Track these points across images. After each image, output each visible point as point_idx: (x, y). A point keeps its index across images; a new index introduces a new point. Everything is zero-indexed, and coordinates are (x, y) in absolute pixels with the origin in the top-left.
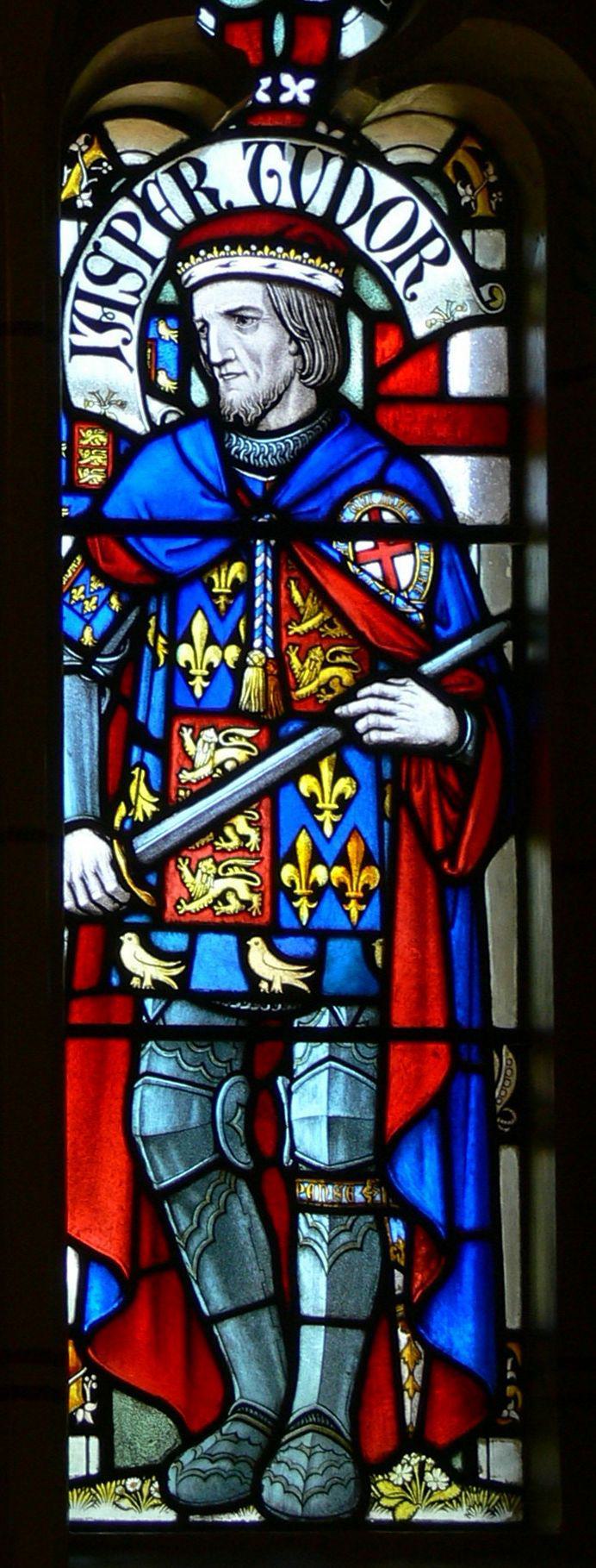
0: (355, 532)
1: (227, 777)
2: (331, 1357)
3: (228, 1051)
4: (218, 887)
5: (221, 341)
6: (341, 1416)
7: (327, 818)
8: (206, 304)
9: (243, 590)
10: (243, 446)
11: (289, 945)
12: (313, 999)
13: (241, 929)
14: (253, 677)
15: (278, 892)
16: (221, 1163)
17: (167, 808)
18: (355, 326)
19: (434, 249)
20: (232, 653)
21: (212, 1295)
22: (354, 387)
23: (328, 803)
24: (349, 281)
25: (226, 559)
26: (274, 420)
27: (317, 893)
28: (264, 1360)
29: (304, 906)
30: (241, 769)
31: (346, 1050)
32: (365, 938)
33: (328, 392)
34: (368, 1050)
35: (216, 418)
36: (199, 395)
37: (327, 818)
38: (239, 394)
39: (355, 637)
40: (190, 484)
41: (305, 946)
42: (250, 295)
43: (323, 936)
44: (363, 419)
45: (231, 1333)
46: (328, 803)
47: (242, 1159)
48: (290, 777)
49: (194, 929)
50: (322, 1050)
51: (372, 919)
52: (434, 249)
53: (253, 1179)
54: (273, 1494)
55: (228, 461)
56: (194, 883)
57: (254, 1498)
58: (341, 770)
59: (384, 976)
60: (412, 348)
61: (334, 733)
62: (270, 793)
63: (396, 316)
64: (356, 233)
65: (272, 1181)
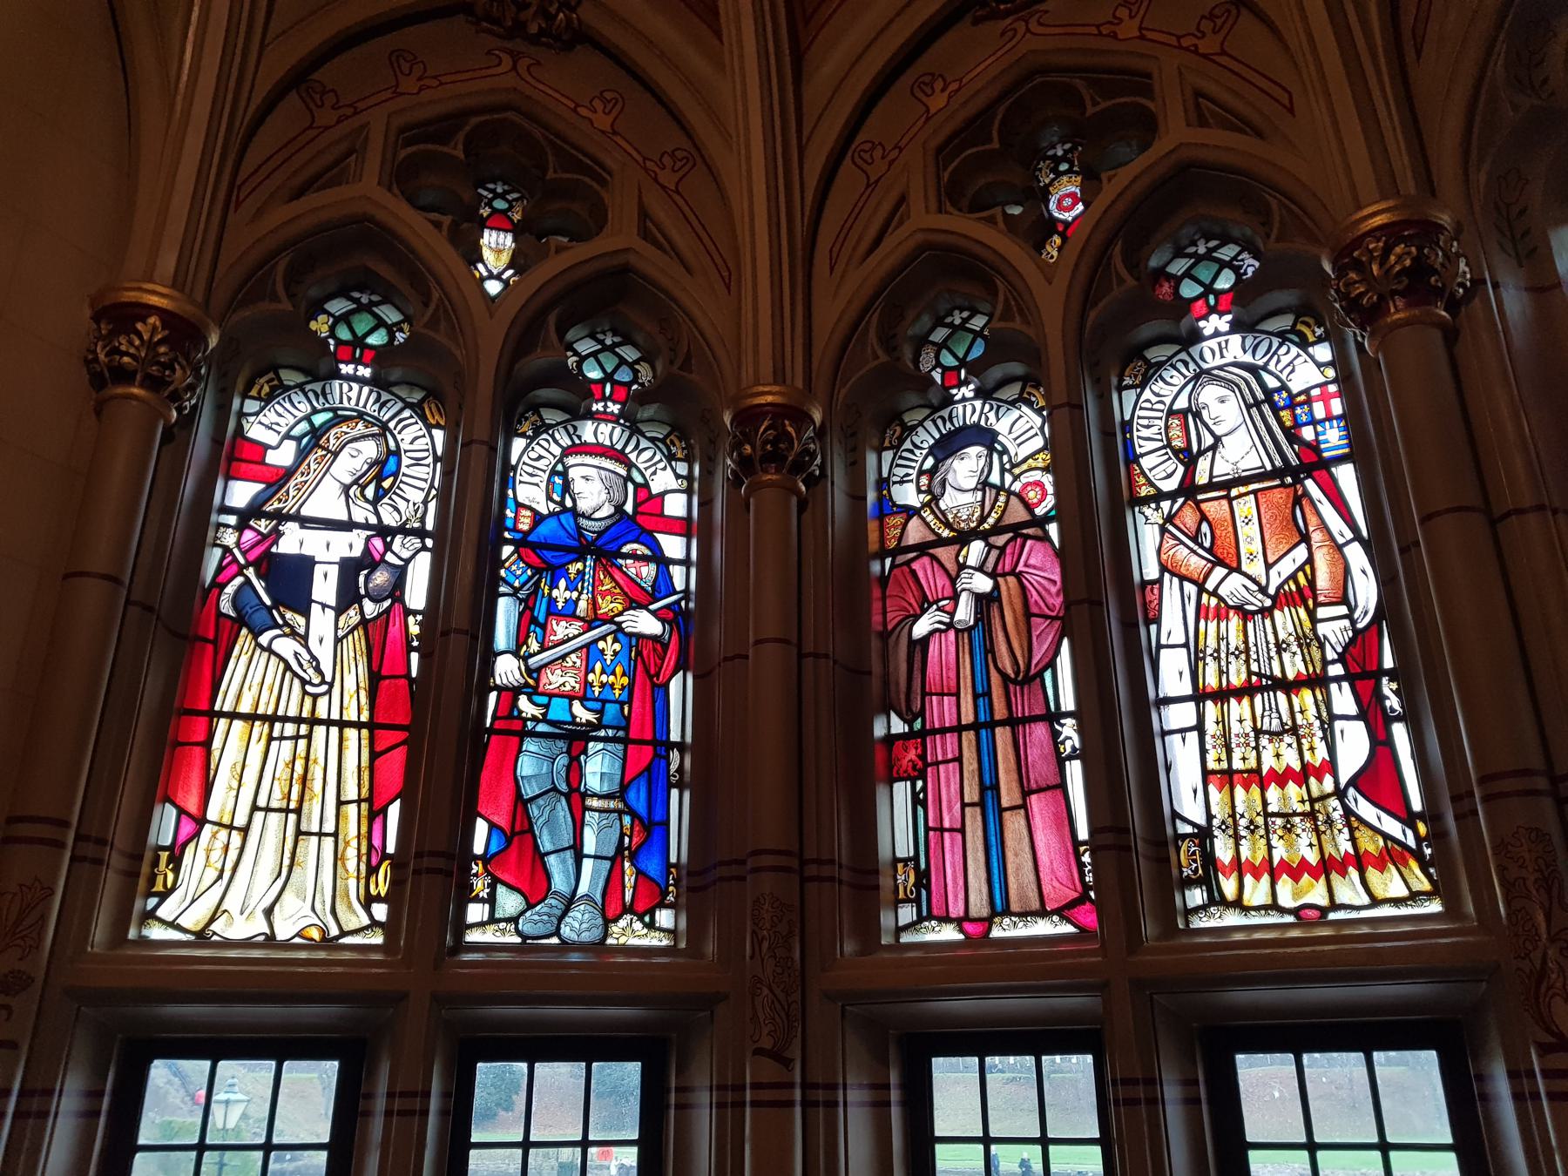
0: (626, 556)
1: (569, 640)
2: (595, 871)
3: (561, 744)
4: (561, 680)
5: (578, 485)
6: (598, 898)
7: (609, 658)
8: (572, 473)
9: (581, 573)
10: (583, 522)
11: (590, 704)
12: (599, 725)
13: (571, 697)
14: (583, 605)
15: (587, 685)
16: (555, 789)
17: (543, 649)
18: (630, 487)
19: (661, 465)
20: (575, 595)
21: (546, 844)
22: (629, 508)
23: (609, 653)
24: (629, 471)
25: (577, 561)
26: (597, 515)
27: (603, 685)
28: (566, 872)
29: (597, 690)
30: (575, 637)
31: (610, 747)
32: (622, 704)
33: (619, 509)
34: (620, 747)
35: (574, 512)
36: (569, 503)
37: (609, 658)
38: (583, 506)
39: (625, 594)
40: (562, 533)
41: (597, 705)
42: (592, 472)
43: (604, 702)
44: (632, 518)
45: (552, 861)
46: (609, 653)
47: (563, 787)
48: (595, 641)
49: (551, 696)
50: (600, 746)
51: (625, 696)
52: (661, 465)
53: (567, 796)
54: (565, 931)
55: (579, 528)
56: (552, 678)
57: (557, 933)
58: (615, 640)
59: (628, 719)
60: (650, 497)
61: (614, 627)
62: (587, 646)
63: (646, 486)
64: (633, 457)
65: (575, 796)
